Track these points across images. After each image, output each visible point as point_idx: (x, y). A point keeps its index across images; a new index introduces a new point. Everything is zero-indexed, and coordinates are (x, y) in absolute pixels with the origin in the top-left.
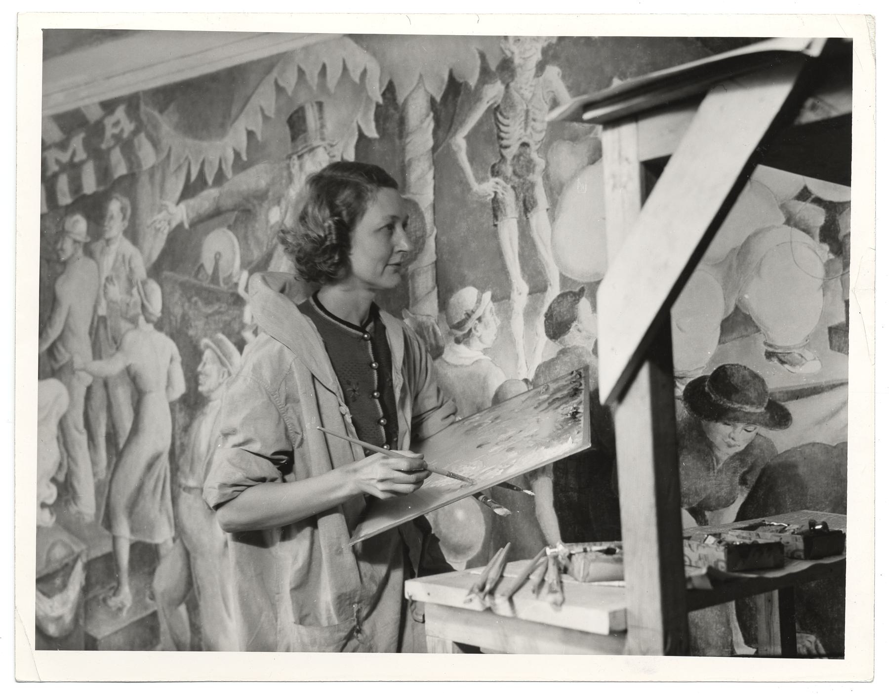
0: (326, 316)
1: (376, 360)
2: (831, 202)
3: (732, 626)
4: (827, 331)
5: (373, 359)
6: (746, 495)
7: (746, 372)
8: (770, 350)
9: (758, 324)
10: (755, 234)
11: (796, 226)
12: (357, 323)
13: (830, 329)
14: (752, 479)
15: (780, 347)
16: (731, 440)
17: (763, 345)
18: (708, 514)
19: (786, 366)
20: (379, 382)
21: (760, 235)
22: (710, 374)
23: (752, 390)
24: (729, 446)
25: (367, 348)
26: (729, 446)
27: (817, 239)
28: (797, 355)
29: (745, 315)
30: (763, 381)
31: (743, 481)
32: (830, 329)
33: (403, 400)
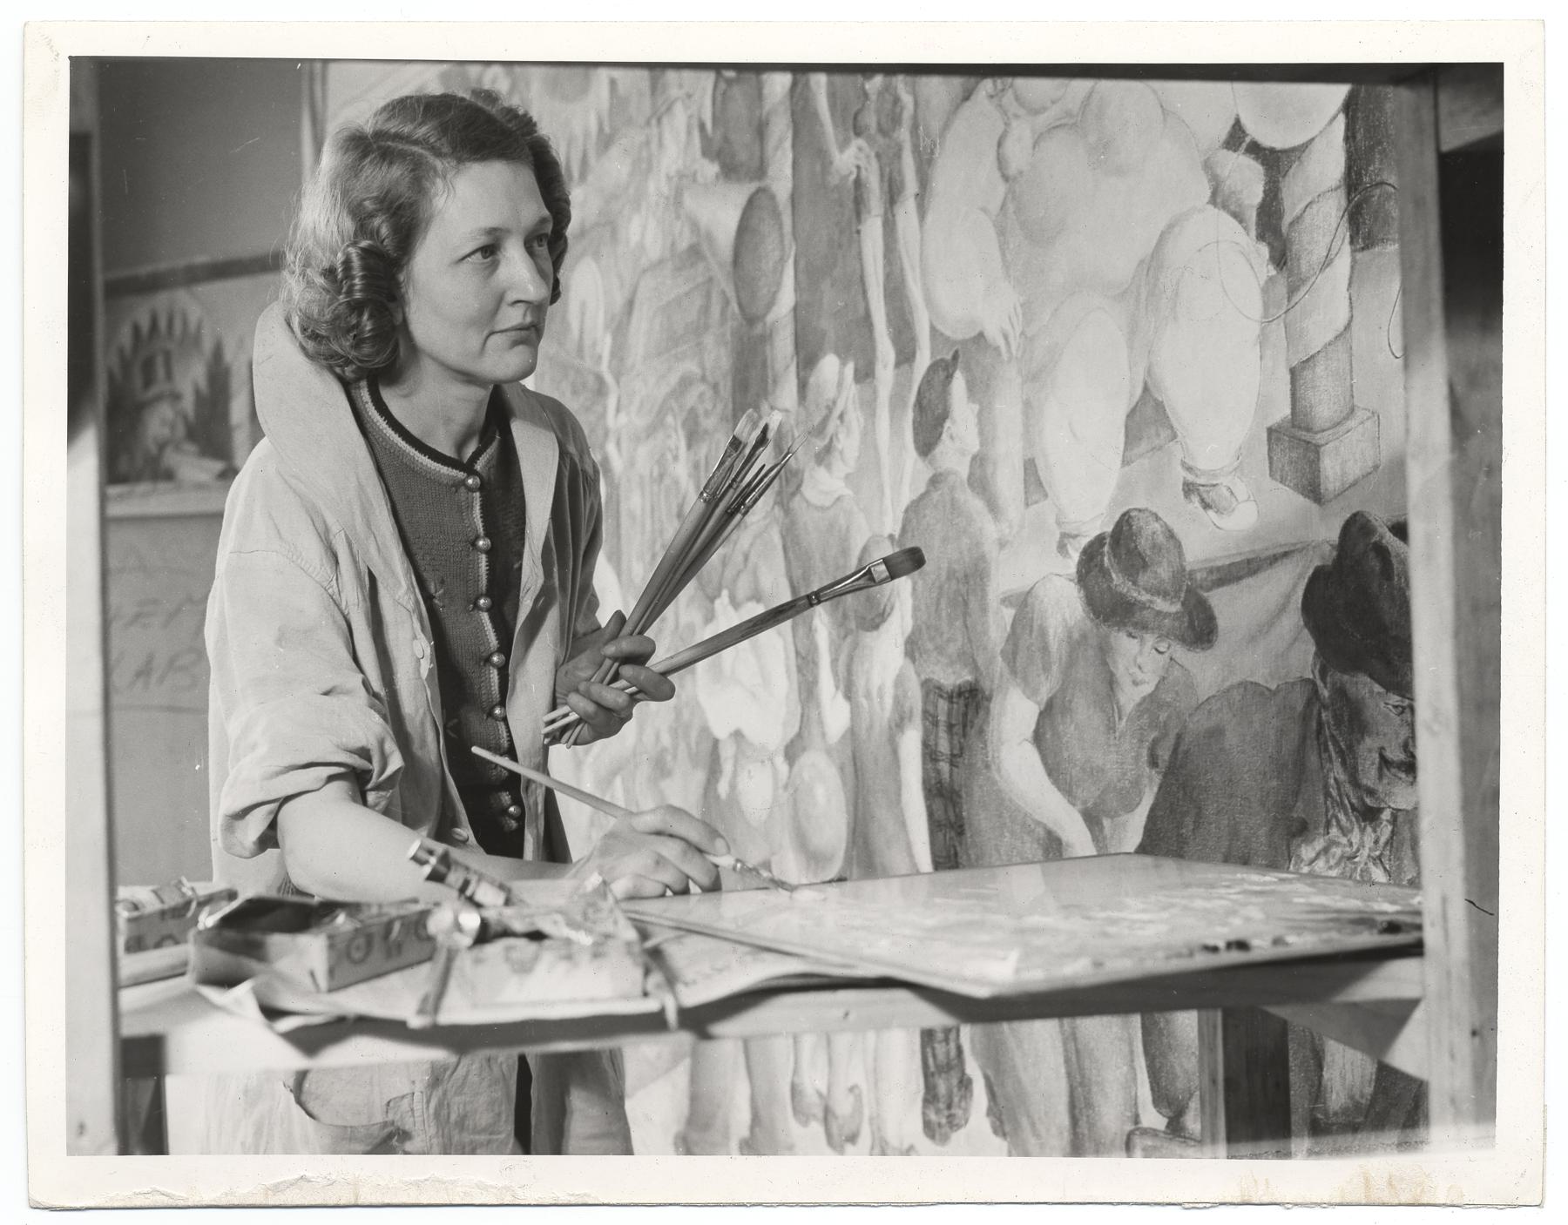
0: (390, 432)
1: (487, 535)
2: (1272, 151)
3: (1136, 1064)
4: (1265, 435)
5: (481, 531)
6: (1155, 789)
7: (1157, 526)
8: (1191, 478)
9: (1176, 425)
10: (1170, 227)
11: (1225, 207)
12: (447, 450)
13: (1270, 431)
14: (1164, 754)
15: (1204, 473)
16: (1136, 670)
17: (1179, 468)
18: (1106, 822)
19: (1211, 513)
20: (489, 581)
21: (1176, 230)
22: (1109, 529)
23: (1165, 564)
24: (1135, 683)
25: (470, 507)
26: (1135, 683)
27: (1253, 233)
28: (1224, 490)
29: (1155, 400)
30: (1180, 546)
31: (1153, 762)
32: (1270, 431)
33: (536, 619)
